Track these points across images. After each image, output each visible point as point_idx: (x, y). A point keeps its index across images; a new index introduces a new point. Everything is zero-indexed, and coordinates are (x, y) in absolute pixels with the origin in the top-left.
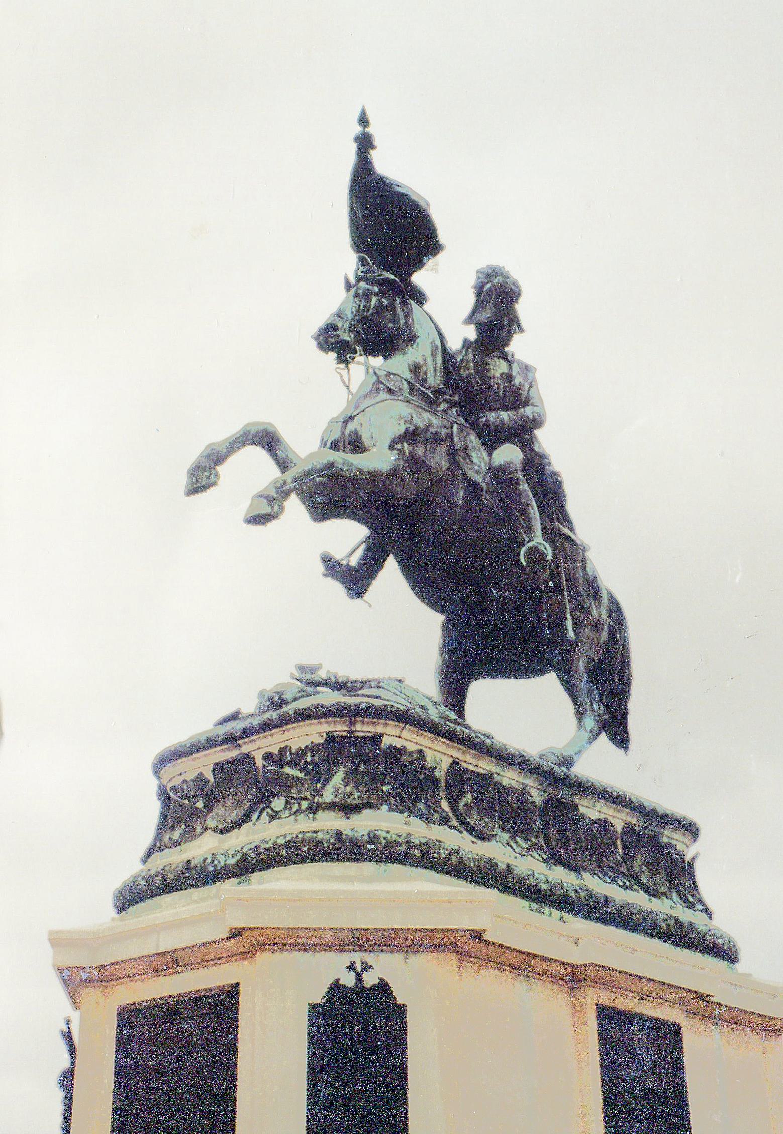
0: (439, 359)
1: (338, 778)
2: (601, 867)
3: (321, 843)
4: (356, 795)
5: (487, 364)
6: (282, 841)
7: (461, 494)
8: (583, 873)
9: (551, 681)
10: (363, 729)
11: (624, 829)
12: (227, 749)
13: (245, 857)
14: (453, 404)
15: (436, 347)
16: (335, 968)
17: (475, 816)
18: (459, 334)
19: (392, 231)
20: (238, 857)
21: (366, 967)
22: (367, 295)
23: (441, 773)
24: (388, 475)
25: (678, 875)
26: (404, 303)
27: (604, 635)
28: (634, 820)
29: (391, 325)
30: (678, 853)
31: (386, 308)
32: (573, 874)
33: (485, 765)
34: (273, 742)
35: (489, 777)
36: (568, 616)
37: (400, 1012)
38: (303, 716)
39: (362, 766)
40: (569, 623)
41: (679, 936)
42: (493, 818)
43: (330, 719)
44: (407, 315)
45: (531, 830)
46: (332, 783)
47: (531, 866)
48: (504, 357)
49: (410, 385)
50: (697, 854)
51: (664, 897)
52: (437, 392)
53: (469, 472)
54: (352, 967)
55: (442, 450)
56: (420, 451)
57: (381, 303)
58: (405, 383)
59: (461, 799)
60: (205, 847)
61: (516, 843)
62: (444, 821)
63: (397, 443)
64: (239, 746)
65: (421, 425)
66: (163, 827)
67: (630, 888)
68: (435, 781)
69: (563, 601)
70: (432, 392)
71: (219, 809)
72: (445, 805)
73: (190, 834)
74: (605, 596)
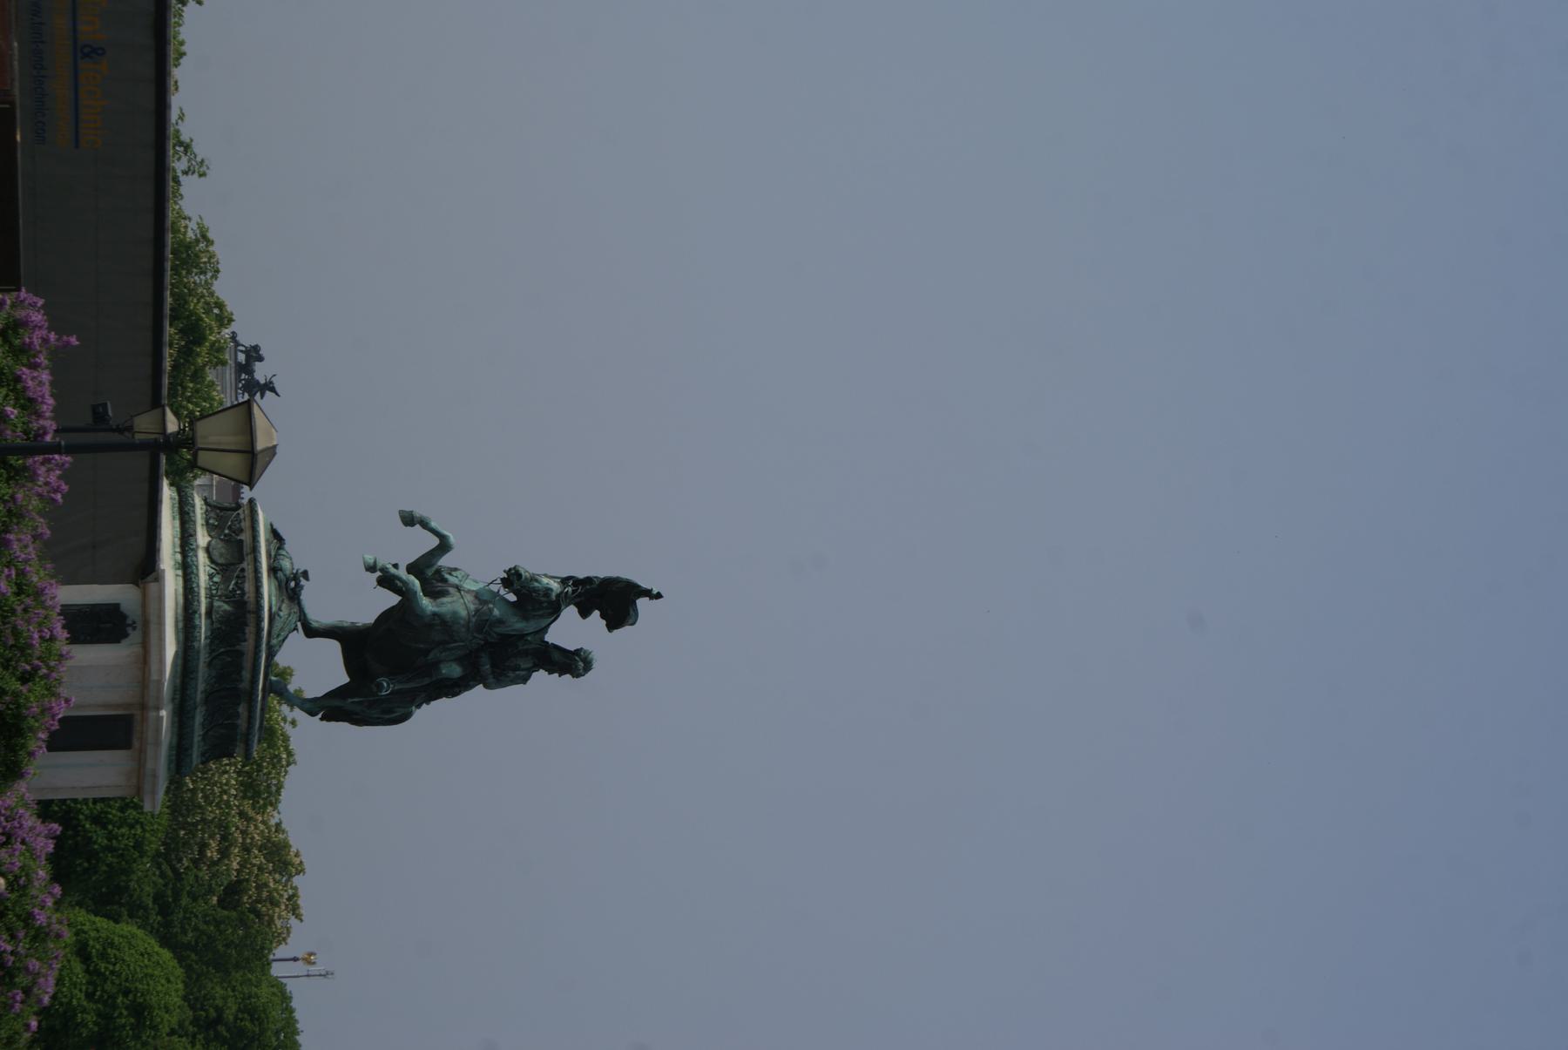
1: (226, 607)
10: (251, 618)
34: (249, 574)
44: (542, 616)
60: (202, 538)
62: (212, 651)
71: (221, 545)
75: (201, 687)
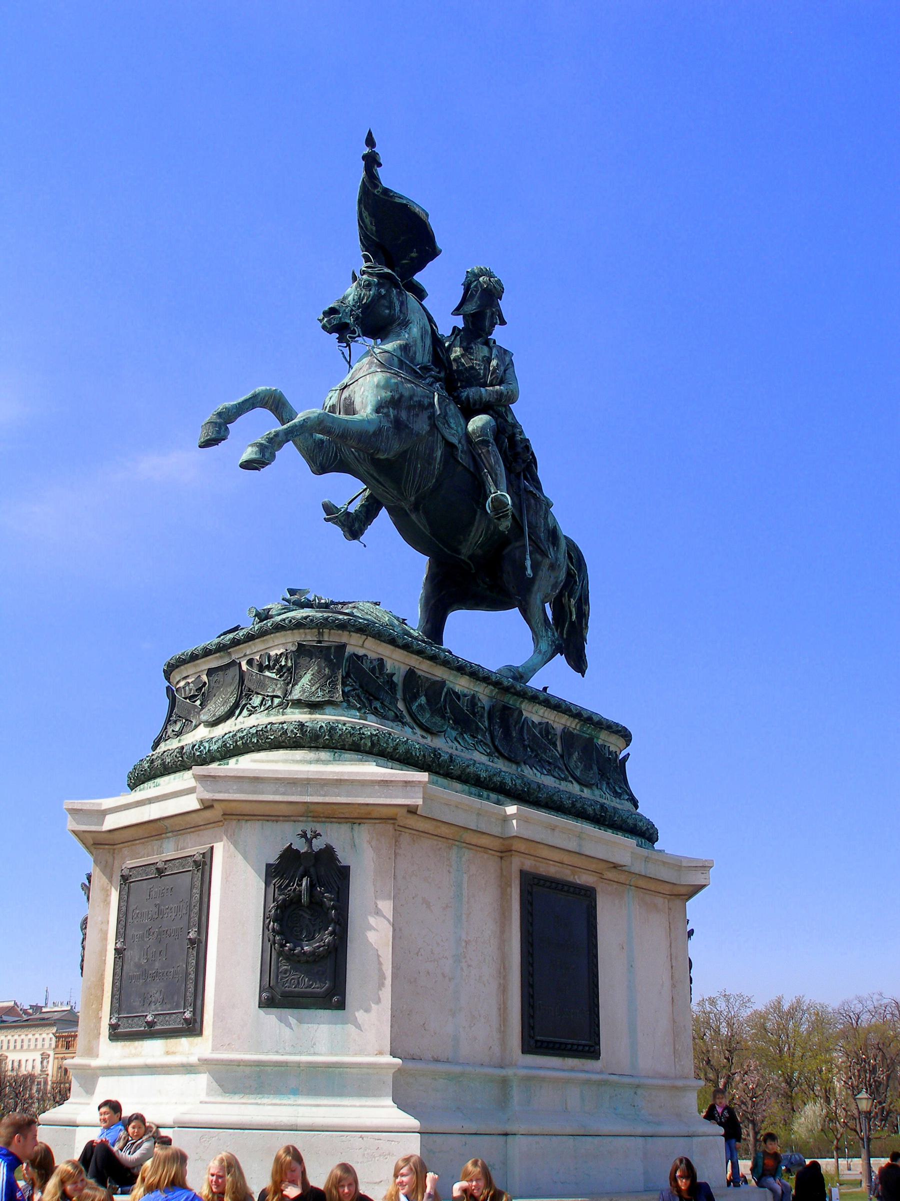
0: (428, 342)
1: (305, 680)
2: (542, 764)
3: (285, 732)
4: (320, 694)
5: (472, 348)
6: (254, 731)
7: (439, 453)
8: (523, 766)
9: (515, 613)
10: (332, 638)
11: (563, 730)
12: (221, 657)
13: (225, 745)
14: (437, 380)
15: (426, 331)
16: (287, 836)
17: (428, 715)
18: (448, 323)
19: (396, 236)
20: (220, 743)
21: (316, 835)
22: (368, 285)
23: (398, 679)
24: (374, 433)
25: (612, 772)
26: (400, 293)
27: (563, 576)
28: (573, 724)
29: (387, 311)
30: (610, 753)
31: (384, 297)
32: (514, 766)
33: (440, 673)
35: (443, 683)
36: (528, 557)
37: (344, 873)
38: (279, 628)
39: (327, 670)
40: (528, 563)
41: (602, 819)
42: (443, 717)
43: (302, 631)
44: (402, 304)
45: (478, 728)
46: (300, 684)
47: (479, 759)
48: (487, 343)
49: (400, 361)
50: (629, 754)
51: (594, 788)
52: (425, 368)
53: (447, 435)
54: (304, 835)
55: (425, 415)
56: (404, 415)
57: (380, 293)
58: (395, 359)
59: (416, 700)
61: (464, 738)
63: (383, 407)
64: (230, 654)
65: (406, 394)
66: (168, 721)
67: (565, 779)
68: (393, 686)
69: (525, 546)
70: (419, 369)
72: (401, 705)
73: (188, 725)
74: (563, 543)
75: (480, 757)
